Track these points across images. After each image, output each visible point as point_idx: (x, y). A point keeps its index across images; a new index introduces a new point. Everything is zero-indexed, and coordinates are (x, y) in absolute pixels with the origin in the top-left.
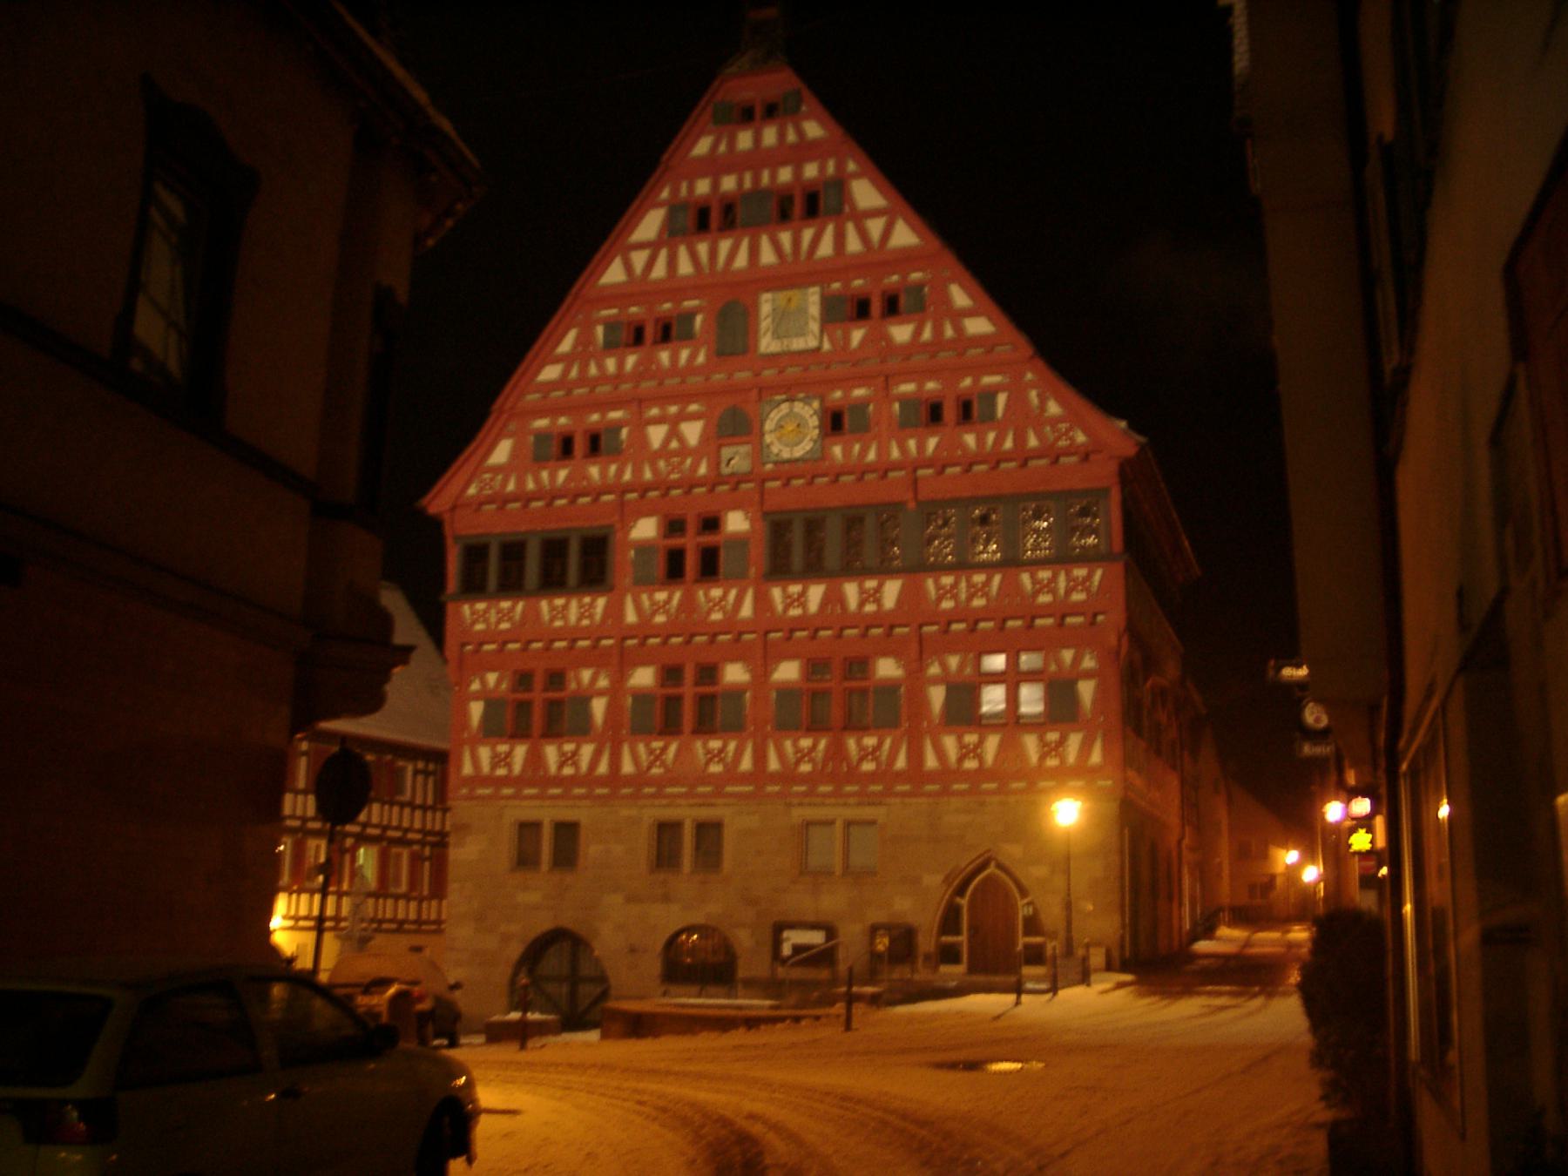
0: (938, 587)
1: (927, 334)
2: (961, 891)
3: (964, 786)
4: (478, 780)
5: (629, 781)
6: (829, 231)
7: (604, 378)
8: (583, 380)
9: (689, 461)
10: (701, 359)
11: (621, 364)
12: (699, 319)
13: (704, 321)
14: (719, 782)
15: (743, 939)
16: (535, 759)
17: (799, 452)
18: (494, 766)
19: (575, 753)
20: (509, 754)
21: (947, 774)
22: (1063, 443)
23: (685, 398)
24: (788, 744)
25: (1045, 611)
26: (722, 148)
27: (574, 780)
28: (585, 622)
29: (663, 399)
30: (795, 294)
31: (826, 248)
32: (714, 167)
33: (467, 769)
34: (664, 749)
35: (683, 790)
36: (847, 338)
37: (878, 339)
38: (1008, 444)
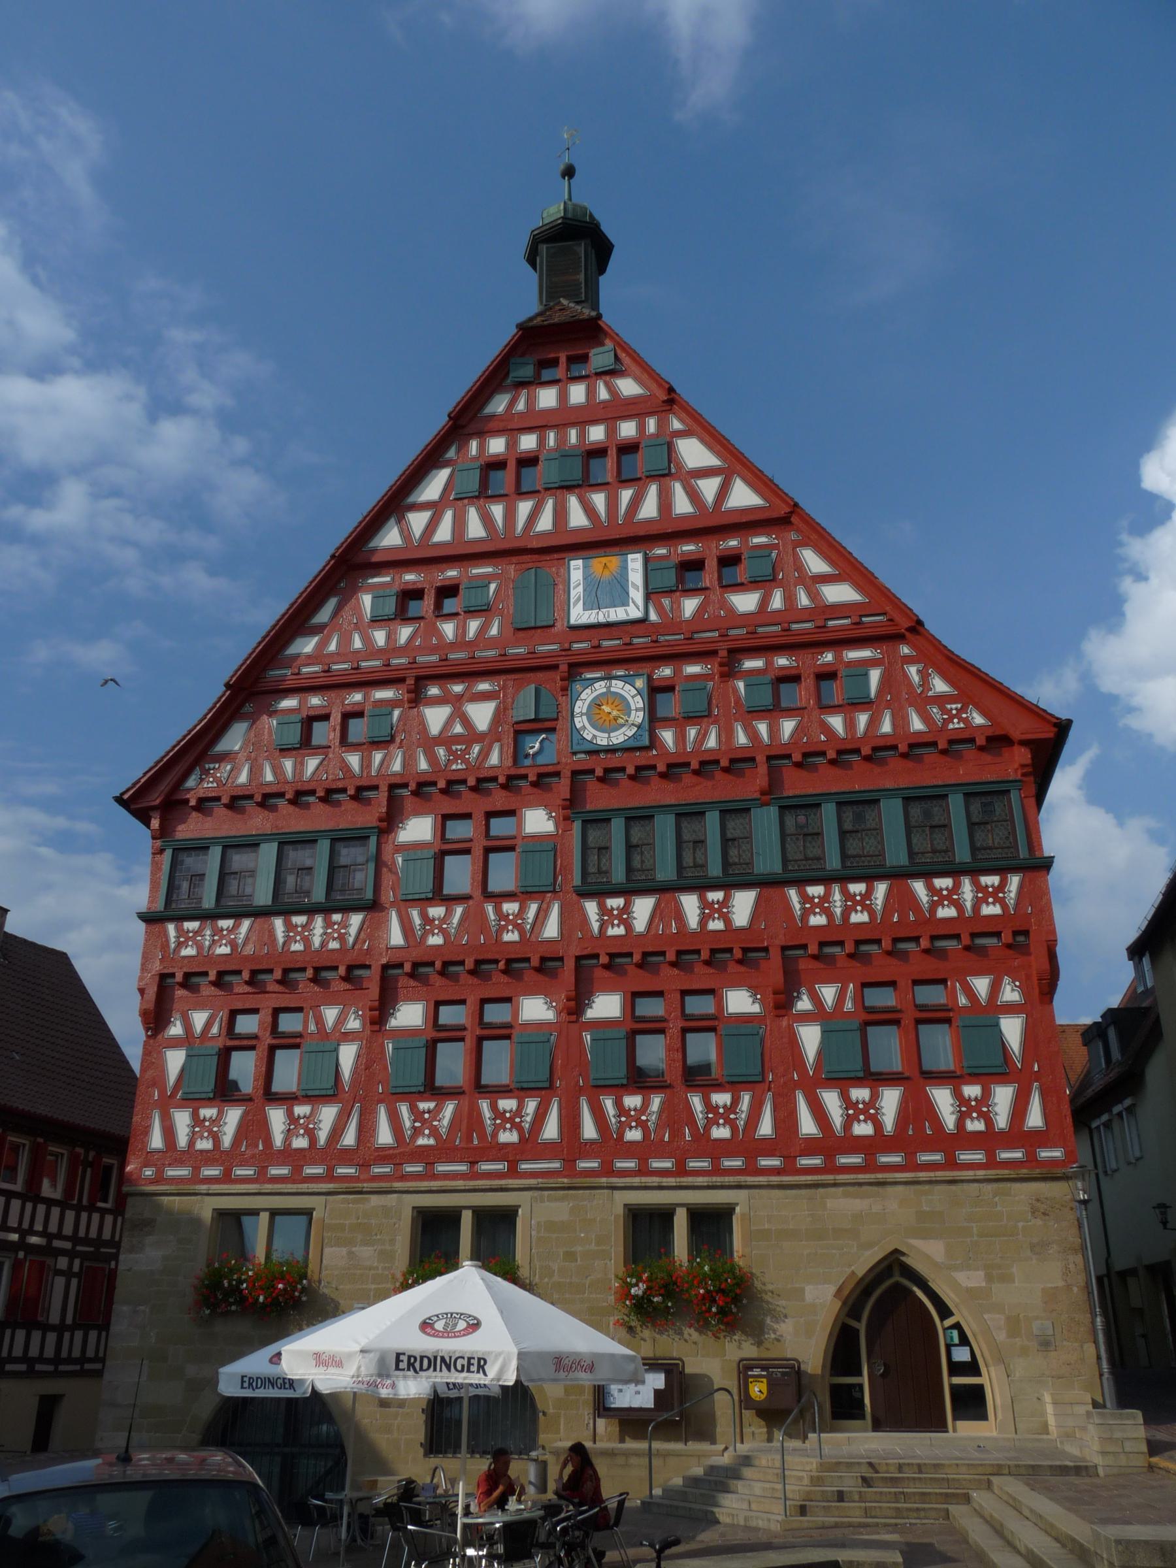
0: (805, 898)
3: (855, 1160)
7: (371, 651)
9: (476, 749)
10: (494, 631)
12: (493, 586)
14: (512, 1156)
17: (618, 738)
21: (830, 1144)
22: (956, 724)
24: (609, 1104)
26: (521, 406)
28: (334, 945)
30: (613, 561)
35: (463, 1168)
36: (678, 608)
38: (886, 727)
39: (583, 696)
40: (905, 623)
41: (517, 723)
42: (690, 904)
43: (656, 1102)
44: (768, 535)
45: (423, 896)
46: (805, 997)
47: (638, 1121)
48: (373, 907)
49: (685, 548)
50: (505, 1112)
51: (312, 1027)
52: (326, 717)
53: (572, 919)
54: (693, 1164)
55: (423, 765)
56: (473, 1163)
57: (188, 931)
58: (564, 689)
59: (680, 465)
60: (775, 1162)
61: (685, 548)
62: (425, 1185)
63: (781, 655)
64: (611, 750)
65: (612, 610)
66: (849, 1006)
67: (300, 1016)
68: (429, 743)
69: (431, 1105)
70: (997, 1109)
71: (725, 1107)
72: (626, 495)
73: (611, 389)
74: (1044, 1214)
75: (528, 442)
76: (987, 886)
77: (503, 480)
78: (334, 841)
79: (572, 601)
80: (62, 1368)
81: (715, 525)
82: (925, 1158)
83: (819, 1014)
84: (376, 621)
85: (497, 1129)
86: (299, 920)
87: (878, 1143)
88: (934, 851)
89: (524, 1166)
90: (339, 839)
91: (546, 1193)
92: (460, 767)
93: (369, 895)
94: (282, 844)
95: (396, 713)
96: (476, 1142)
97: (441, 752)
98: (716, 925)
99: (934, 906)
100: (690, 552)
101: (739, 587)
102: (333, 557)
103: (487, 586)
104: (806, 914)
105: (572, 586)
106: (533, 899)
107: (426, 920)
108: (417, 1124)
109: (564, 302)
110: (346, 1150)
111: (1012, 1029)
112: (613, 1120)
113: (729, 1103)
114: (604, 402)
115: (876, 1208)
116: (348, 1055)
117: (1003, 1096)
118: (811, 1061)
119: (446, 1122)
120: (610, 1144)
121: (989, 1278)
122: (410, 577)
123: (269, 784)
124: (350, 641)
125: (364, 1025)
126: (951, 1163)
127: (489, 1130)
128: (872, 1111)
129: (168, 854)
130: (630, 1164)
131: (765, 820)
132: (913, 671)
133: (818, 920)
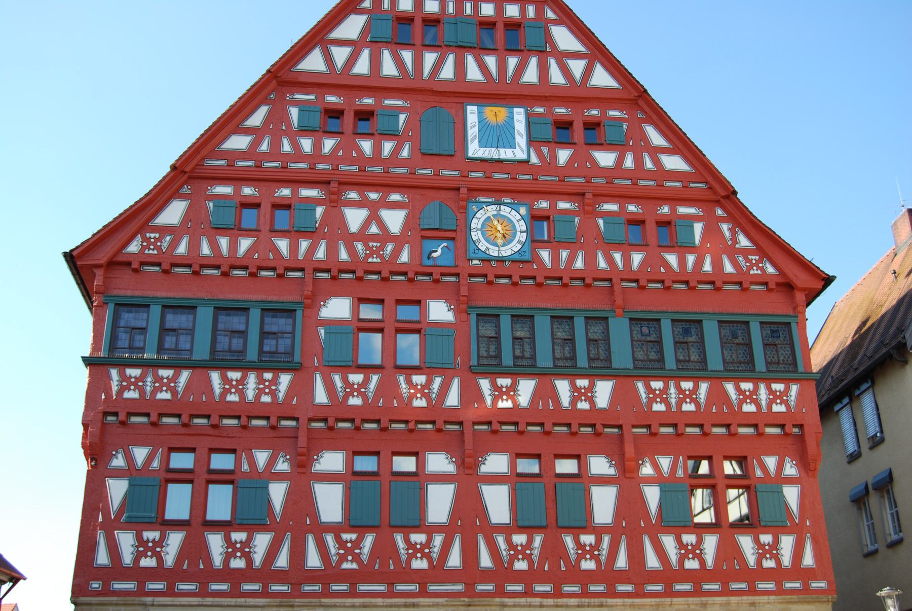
5: (313, 576)
9: (390, 248)
23: (386, 185)
34: (357, 543)
35: (381, 588)
43: (538, 540)
46: (648, 465)
50: (416, 544)
56: (391, 584)
59: (554, 45)
62: (349, 601)
68: (350, 239)
71: (590, 545)
72: (513, 62)
76: (776, 391)
83: (658, 479)
85: (410, 557)
89: (433, 588)
92: (375, 260)
96: (392, 567)
97: (360, 246)
112: (504, 553)
113: (593, 543)
118: (653, 512)
127: (404, 558)
130: (519, 588)
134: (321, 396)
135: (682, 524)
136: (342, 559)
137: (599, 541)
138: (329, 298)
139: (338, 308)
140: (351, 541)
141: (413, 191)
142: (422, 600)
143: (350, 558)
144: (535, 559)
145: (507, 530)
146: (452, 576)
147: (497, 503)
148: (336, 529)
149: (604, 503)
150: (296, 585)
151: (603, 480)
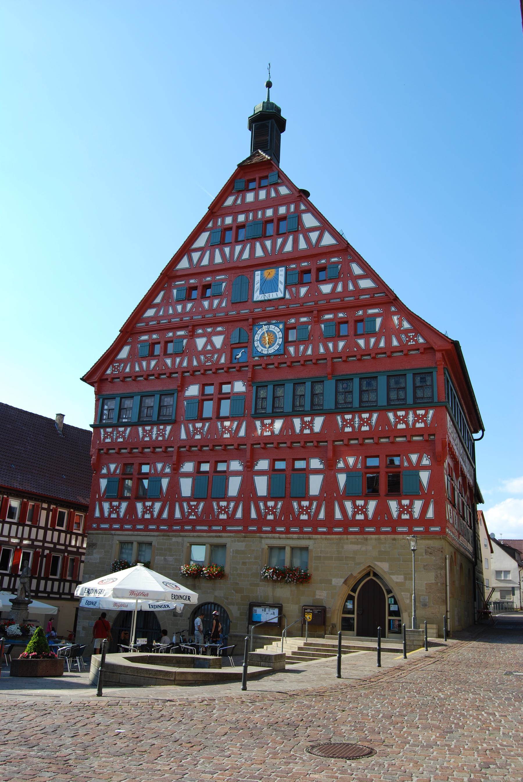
0: (344, 420)
1: (340, 289)
2: (354, 590)
3: (356, 529)
4: (102, 519)
5: (177, 522)
6: (291, 238)
7: (176, 314)
8: (166, 315)
9: (216, 356)
10: (224, 305)
11: (184, 308)
12: (224, 284)
13: (226, 287)
14: (224, 524)
15: (235, 612)
16: (131, 510)
17: (271, 351)
18: (110, 513)
19: (152, 507)
20: (119, 507)
21: (347, 523)
22: (412, 343)
23: (214, 323)
25: (402, 433)
26: (239, 202)
27: (152, 521)
28: (160, 438)
29: (204, 325)
30: (273, 271)
31: (289, 247)
32: (234, 211)
33: (97, 514)
34: (197, 506)
35: (206, 528)
36: (298, 292)
37: (314, 290)
38: (382, 344)
39: (258, 332)
40: (392, 298)
41: (232, 344)
42: (297, 422)
43: (280, 504)
44: (338, 257)
45: (193, 419)
46: (341, 462)
47: (272, 511)
48: (174, 422)
49: (303, 264)
50: (222, 506)
51: (153, 471)
52: (159, 343)
53: (251, 428)
54: (292, 529)
55: (195, 363)
56: (210, 526)
57: (108, 432)
58: (251, 329)
60: (324, 530)
61: (303, 264)
63: (341, 312)
64: (269, 356)
65: (271, 294)
66: (359, 466)
67: (149, 466)
68: (198, 354)
69: (195, 503)
70: (414, 510)
71: (306, 507)
73: (277, 192)
74: (430, 553)
75: (241, 218)
77: (229, 236)
78: (161, 395)
79: (255, 290)
80: (63, 596)
81: (316, 253)
82: (384, 529)
83: (347, 470)
84: (179, 301)
85: (220, 513)
86: (148, 428)
87: (366, 522)
88: (398, 399)
90: (163, 394)
91: (237, 539)
92: (209, 364)
93: (173, 418)
94: (142, 397)
95: (185, 341)
97: (202, 357)
98: (307, 431)
99: (397, 423)
100: (305, 266)
101: (325, 282)
102: (161, 274)
103: (222, 284)
104: (344, 426)
105: (256, 283)
106: (235, 420)
107: (195, 428)
108: (190, 511)
109: (260, 151)
110: (164, 520)
111: (424, 476)
112: (263, 511)
114: (273, 198)
115: (364, 548)
116: (165, 482)
117: (418, 504)
119: (200, 510)
120: (261, 520)
121: (405, 579)
122: (192, 281)
123: (137, 372)
124: (168, 310)
125: (171, 470)
126: (394, 532)
127: (216, 513)
128: (364, 510)
129: (101, 400)
130: (268, 529)
131: (330, 385)
132: (395, 319)
133: (348, 430)
134: (183, 436)
135: (357, 495)
136: (190, 514)
137: (311, 504)
138: (189, 386)
139: (193, 390)
140: (194, 506)
141: (227, 324)
142: (223, 534)
143: (193, 514)
144: (278, 514)
145: (265, 499)
146: (237, 522)
147: (261, 485)
148: (187, 500)
149: (315, 484)
150: (170, 526)
151: (316, 472)
